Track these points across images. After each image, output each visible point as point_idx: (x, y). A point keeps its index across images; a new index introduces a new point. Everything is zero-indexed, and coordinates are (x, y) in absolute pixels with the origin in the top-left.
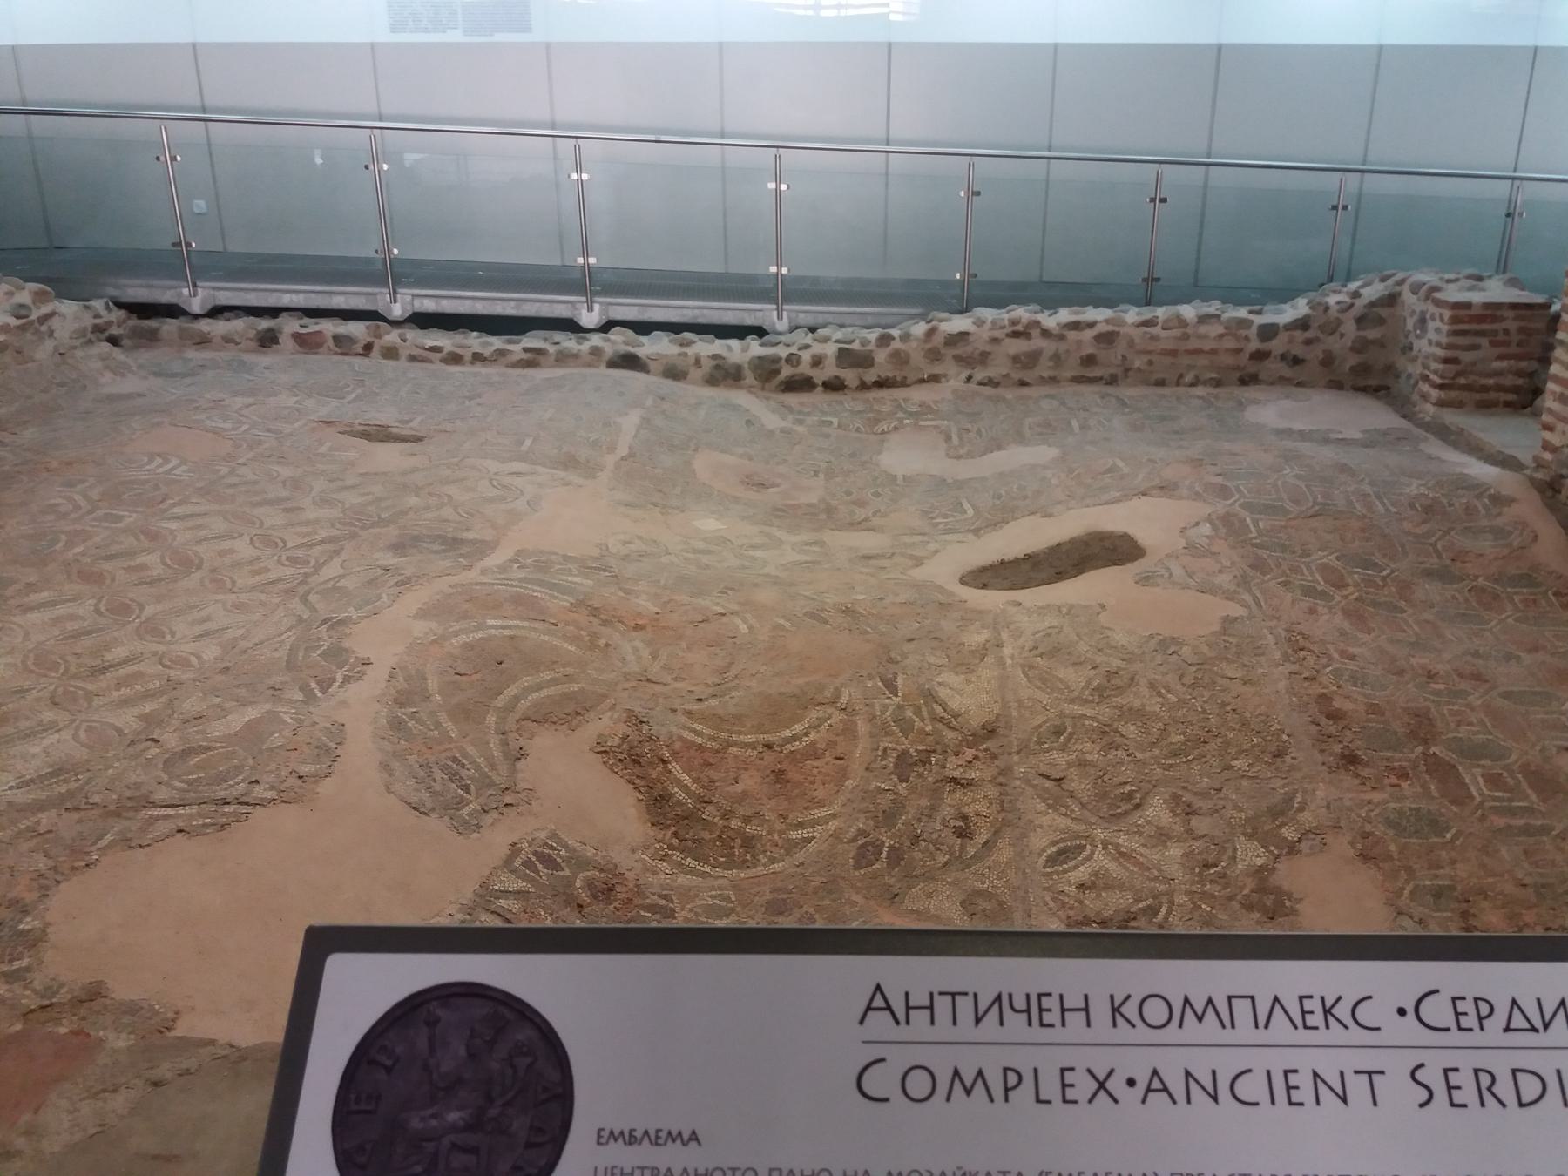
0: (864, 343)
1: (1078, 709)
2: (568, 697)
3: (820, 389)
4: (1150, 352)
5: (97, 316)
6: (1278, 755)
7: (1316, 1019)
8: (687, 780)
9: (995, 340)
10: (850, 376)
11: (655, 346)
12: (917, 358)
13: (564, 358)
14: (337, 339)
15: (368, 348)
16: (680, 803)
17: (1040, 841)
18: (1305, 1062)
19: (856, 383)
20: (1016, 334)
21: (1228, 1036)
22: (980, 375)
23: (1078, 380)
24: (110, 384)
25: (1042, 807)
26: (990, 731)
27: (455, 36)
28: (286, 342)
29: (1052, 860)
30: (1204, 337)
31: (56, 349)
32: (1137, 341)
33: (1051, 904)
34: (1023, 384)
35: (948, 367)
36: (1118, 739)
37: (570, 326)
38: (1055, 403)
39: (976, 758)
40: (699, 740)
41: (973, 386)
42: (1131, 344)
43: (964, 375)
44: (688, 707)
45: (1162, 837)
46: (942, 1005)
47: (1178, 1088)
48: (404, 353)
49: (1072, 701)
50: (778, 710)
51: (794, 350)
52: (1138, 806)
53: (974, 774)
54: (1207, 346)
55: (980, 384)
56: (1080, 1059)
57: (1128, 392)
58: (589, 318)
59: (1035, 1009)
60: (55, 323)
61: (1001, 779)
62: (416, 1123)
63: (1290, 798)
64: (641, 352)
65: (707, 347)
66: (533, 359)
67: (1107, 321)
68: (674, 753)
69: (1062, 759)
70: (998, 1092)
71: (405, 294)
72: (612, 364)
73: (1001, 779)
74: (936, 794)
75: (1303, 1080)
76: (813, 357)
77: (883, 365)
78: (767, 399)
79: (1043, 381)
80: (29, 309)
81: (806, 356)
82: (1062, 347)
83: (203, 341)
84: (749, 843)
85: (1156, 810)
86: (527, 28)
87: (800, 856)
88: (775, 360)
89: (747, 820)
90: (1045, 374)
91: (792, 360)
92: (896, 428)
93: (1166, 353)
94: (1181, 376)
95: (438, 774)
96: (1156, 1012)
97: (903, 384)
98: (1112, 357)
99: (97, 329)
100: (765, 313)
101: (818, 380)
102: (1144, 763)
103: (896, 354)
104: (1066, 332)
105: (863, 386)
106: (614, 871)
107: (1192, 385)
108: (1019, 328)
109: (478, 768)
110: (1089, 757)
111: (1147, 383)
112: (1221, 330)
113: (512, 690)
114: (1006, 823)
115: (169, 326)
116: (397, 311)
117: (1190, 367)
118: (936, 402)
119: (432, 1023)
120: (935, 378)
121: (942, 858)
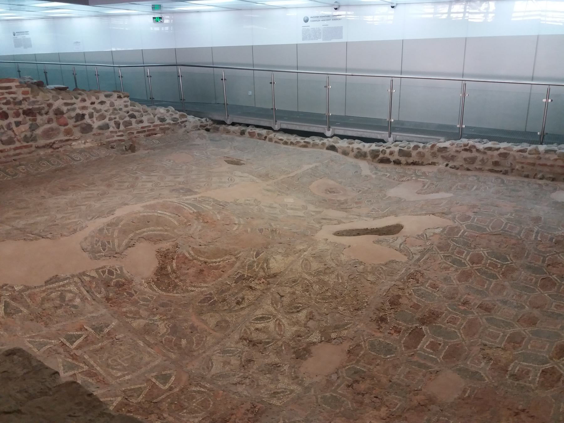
0: (409, 148)
1: (306, 276)
2: (161, 235)
3: (392, 163)
4: (522, 163)
5: (202, 122)
6: (358, 310)
8: (174, 265)
9: (457, 151)
10: (403, 159)
11: (343, 144)
12: (428, 155)
13: (315, 145)
14: (259, 134)
15: (266, 137)
16: (167, 271)
17: (259, 313)
19: (405, 162)
20: (466, 150)
22: (451, 164)
23: (491, 171)
24: (198, 141)
25: (269, 302)
26: (275, 276)
27: (320, 41)
28: (247, 133)
29: (257, 319)
30: (548, 159)
31: (186, 130)
32: (517, 157)
33: (243, 331)
34: (468, 170)
35: (439, 160)
36: (310, 289)
37: (322, 135)
38: (475, 178)
39: (263, 282)
40: (188, 255)
41: (448, 168)
42: (514, 157)
43: (445, 163)
44: (195, 247)
45: (297, 323)
48: (274, 140)
49: (307, 273)
50: (218, 253)
51: (385, 148)
52: (298, 312)
53: (258, 287)
54: (549, 163)
55: (451, 167)
57: (510, 178)
58: (328, 134)
60: (187, 123)
61: (265, 291)
63: (347, 324)
64: (337, 145)
65: (357, 145)
66: (306, 145)
67: (505, 149)
68: (178, 257)
69: (288, 290)
71: (279, 122)
72: (328, 149)
73: (265, 291)
74: (242, 289)
76: (390, 151)
77: (414, 157)
78: (372, 165)
79: (477, 169)
80: (178, 119)
81: (388, 151)
82: (485, 157)
83: (228, 132)
84: (176, 286)
85: (302, 315)
86: (341, 38)
87: (185, 295)
88: (378, 151)
89: (181, 281)
90: (477, 167)
91: (384, 152)
92: (408, 180)
93: (529, 164)
94: (536, 175)
95: (100, 244)
97: (422, 164)
98: (507, 163)
99: (201, 126)
100: (382, 135)
101: (392, 160)
102: (311, 298)
103: (419, 153)
104: (486, 151)
105: (407, 164)
106: (130, 281)
107: (541, 179)
108: (467, 147)
109: (114, 245)
110: (297, 292)
111: (520, 175)
112: (556, 157)
113: (145, 230)
114: (254, 304)
115: (222, 127)
116: (276, 127)
117: (540, 171)
118: (429, 172)
120: (433, 164)
121: (226, 308)
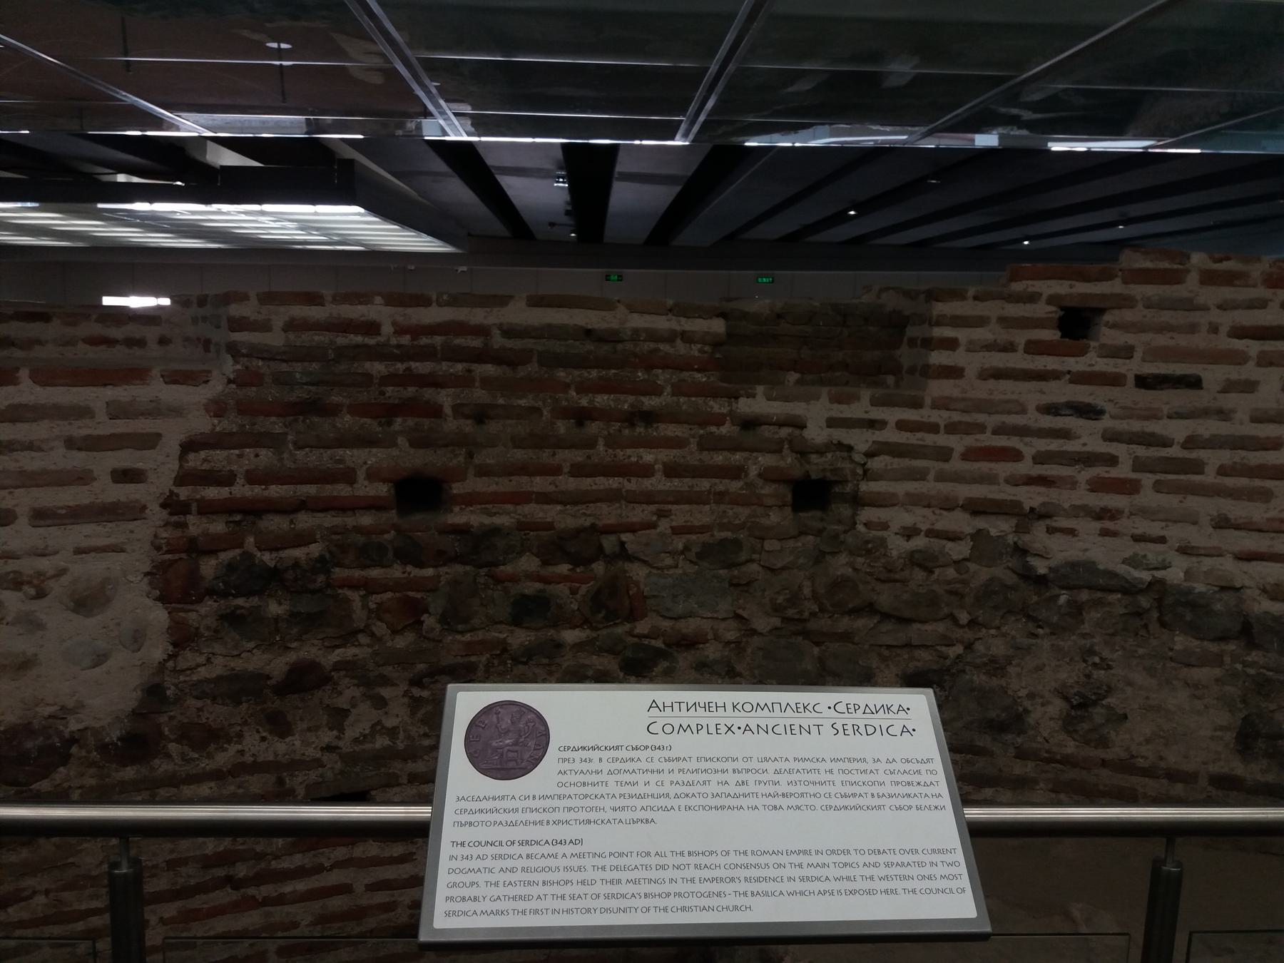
7: (801, 710)
18: (797, 722)
21: (772, 714)
46: (676, 706)
47: (755, 729)
56: (722, 721)
59: (707, 707)
62: (494, 744)
70: (695, 730)
75: (796, 728)
96: (747, 707)
119: (497, 713)
